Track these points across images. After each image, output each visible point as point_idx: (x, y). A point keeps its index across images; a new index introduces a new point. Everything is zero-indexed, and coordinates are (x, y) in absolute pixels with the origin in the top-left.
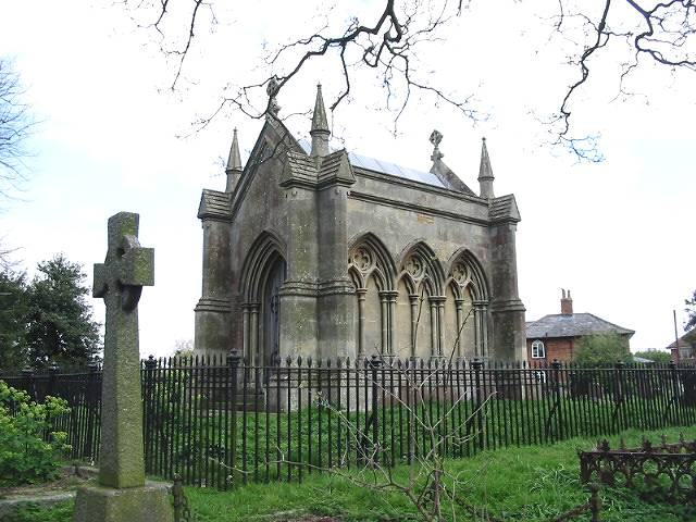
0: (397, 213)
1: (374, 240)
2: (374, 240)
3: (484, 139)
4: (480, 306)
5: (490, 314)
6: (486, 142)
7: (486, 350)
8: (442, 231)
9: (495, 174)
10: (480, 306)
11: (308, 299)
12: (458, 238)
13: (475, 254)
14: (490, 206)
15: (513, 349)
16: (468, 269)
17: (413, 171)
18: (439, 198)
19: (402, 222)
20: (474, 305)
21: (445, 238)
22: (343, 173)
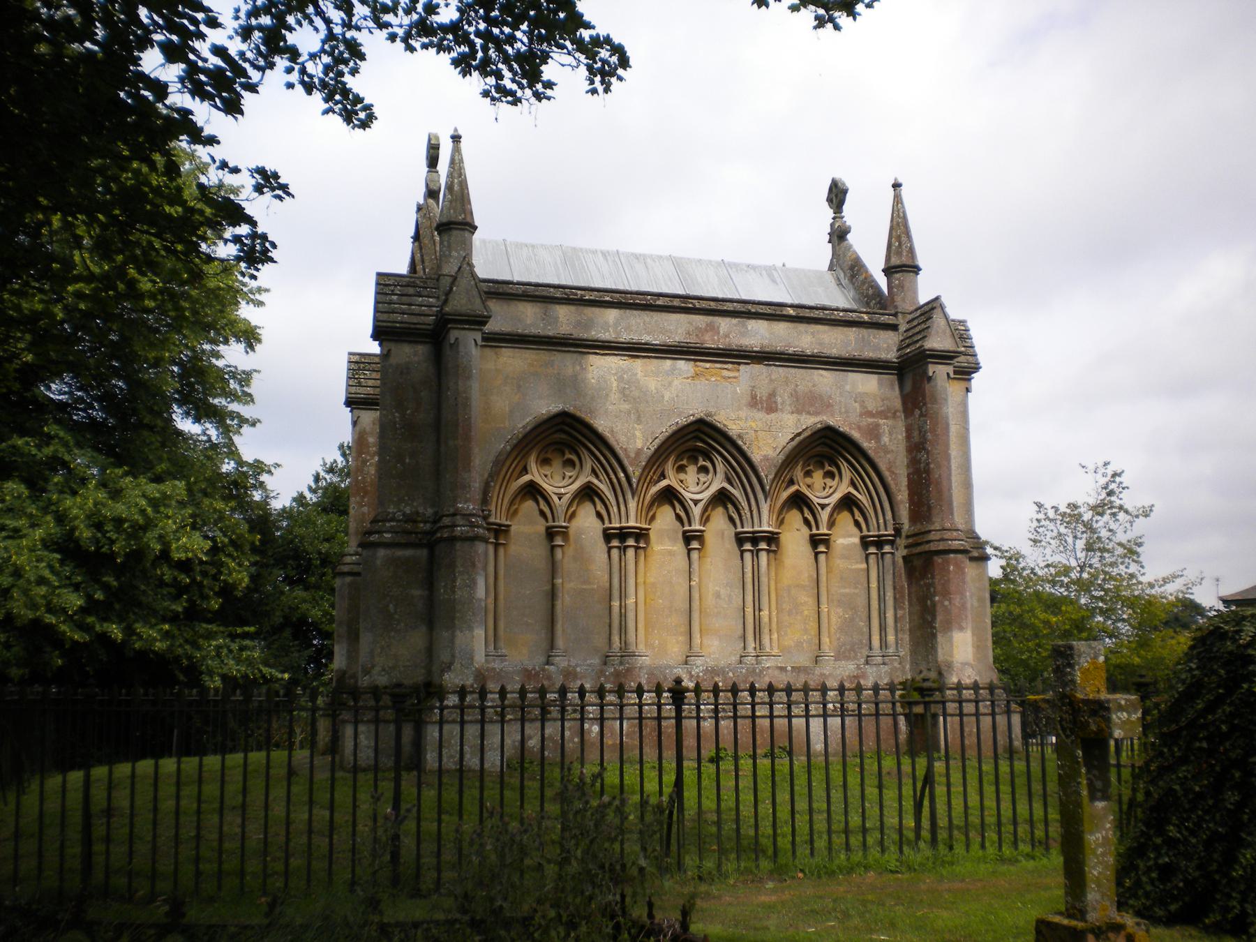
0: (639, 367)
1: (579, 426)
2: (579, 426)
3: (896, 186)
4: (879, 544)
5: (900, 561)
6: (904, 191)
7: (891, 638)
8: (763, 392)
9: (921, 261)
10: (879, 544)
11: (408, 553)
12: (805, 403)
13: (856, 435)
14: (903, 328)
15: (934, 636)
16: (844, 467)
17: (770, 272)
18: (753, 324)
19: (652, 384)
20: (865, 543)
21: (771, 407)
22: (461, 302)
